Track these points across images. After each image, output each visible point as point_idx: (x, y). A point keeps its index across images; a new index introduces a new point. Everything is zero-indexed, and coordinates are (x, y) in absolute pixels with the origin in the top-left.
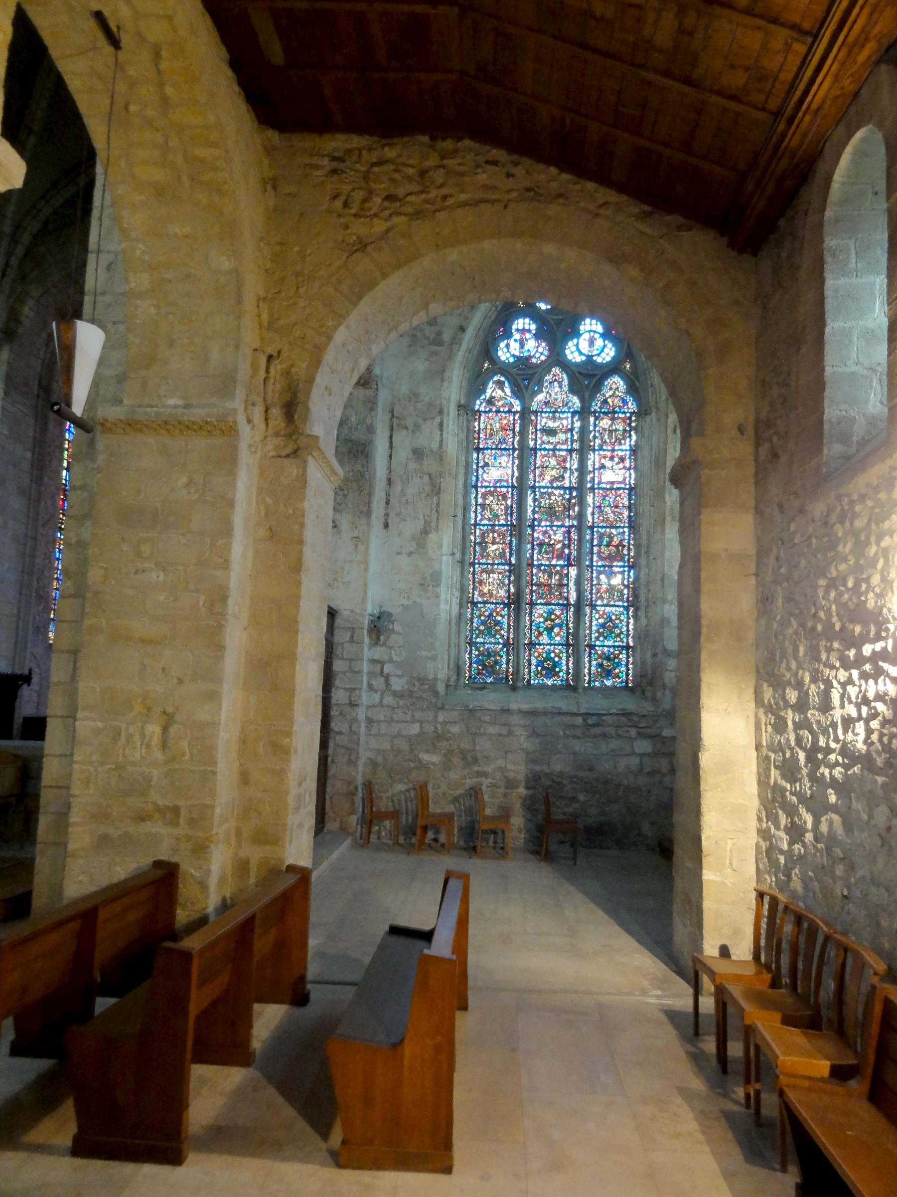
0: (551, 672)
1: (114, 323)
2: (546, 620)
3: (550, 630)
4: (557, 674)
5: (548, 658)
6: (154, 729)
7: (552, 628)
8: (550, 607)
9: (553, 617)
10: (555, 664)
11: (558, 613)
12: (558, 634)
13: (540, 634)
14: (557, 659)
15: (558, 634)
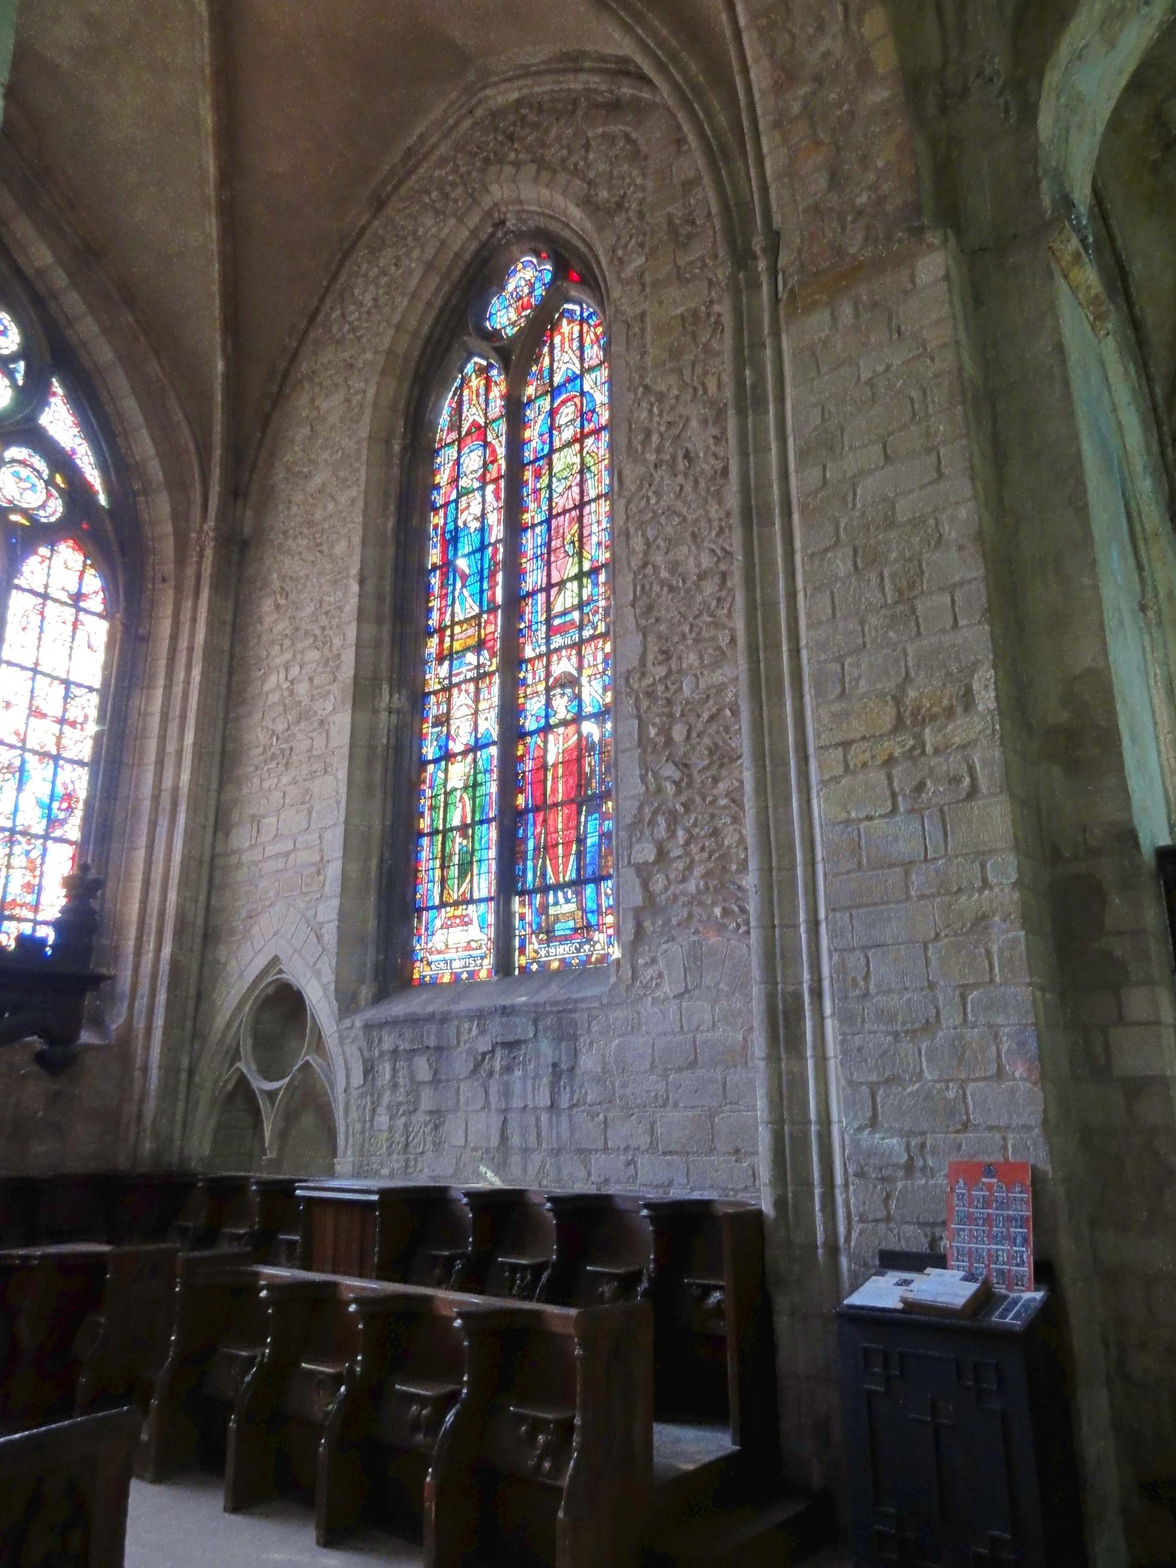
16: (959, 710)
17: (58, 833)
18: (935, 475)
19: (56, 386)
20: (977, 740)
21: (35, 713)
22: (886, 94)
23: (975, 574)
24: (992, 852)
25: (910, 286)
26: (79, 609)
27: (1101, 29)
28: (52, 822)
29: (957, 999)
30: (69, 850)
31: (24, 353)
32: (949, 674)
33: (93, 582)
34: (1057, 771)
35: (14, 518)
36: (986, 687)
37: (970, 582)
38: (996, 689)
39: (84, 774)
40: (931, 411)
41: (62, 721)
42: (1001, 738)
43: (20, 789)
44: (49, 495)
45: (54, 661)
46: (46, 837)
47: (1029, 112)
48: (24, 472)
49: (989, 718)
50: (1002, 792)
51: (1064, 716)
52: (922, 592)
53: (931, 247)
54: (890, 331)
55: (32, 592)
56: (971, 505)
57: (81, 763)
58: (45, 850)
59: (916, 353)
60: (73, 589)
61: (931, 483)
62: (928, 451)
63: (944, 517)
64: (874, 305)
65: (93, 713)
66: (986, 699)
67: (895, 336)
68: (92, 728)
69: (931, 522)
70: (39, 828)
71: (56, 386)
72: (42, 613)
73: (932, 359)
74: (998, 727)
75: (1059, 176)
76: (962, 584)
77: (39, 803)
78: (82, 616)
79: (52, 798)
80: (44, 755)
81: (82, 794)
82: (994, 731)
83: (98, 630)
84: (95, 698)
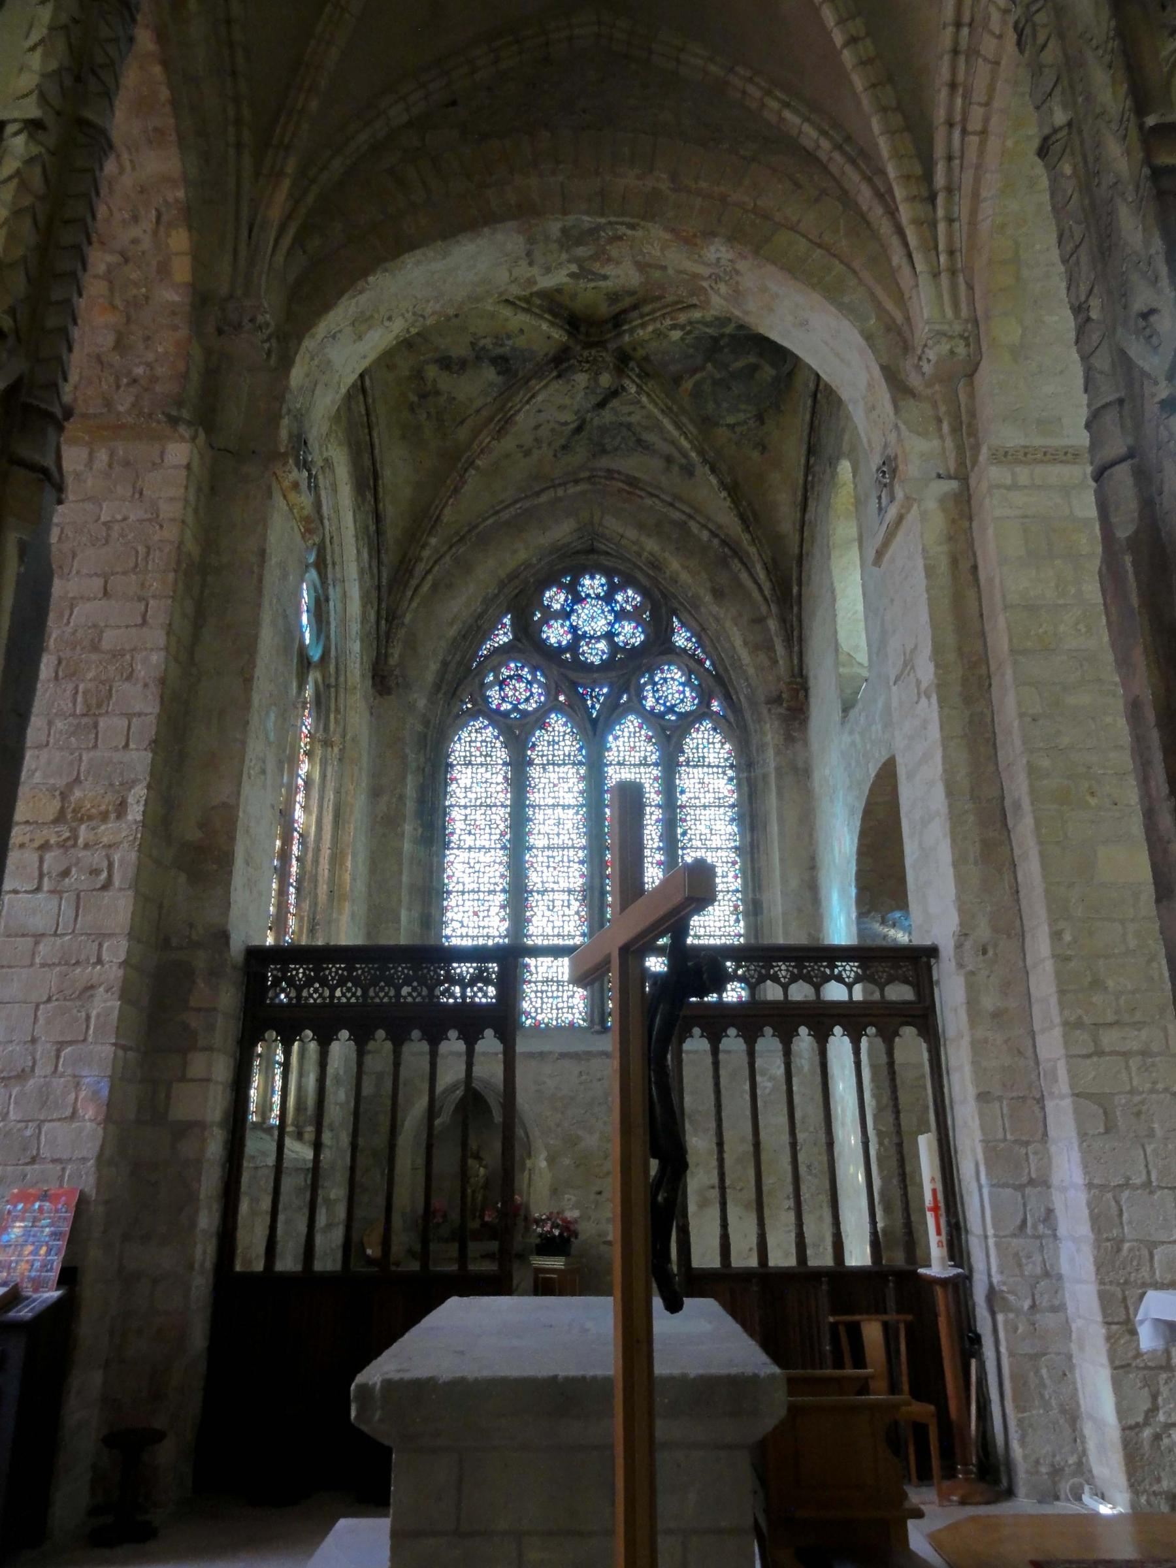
16: (113, 816)
18: (139, 621)
20: (121, 842)
22: (177, 298)
23: (150, 710)
24: (111, 935)
25: (158, 461)
27: (353, 324)
29: (53, 1054)
32: (111, 785)
34: (183, 878)
36: (138, 802)
37: (146, 715)
38: (146, 804)
40: (150, 568)
42: (140, 845)
47: (286, 362)
49: (134, 827)
50: (130, 888)
51: (199, 834)
52: (107, 712)
53: (182, 439)
54: (134, 488)
56: (163, 654)
59: (149, 516)
61: (136, 625)
62: (140, 599)
63: (139, 657)
64: (127, 463)
66: (135, 813)
67: (137, 496)
69: (128, 657)
73: (161, 527)
74: (139, 836)
75: (299, 417)
76: (140, 715)
82: (135, 838)
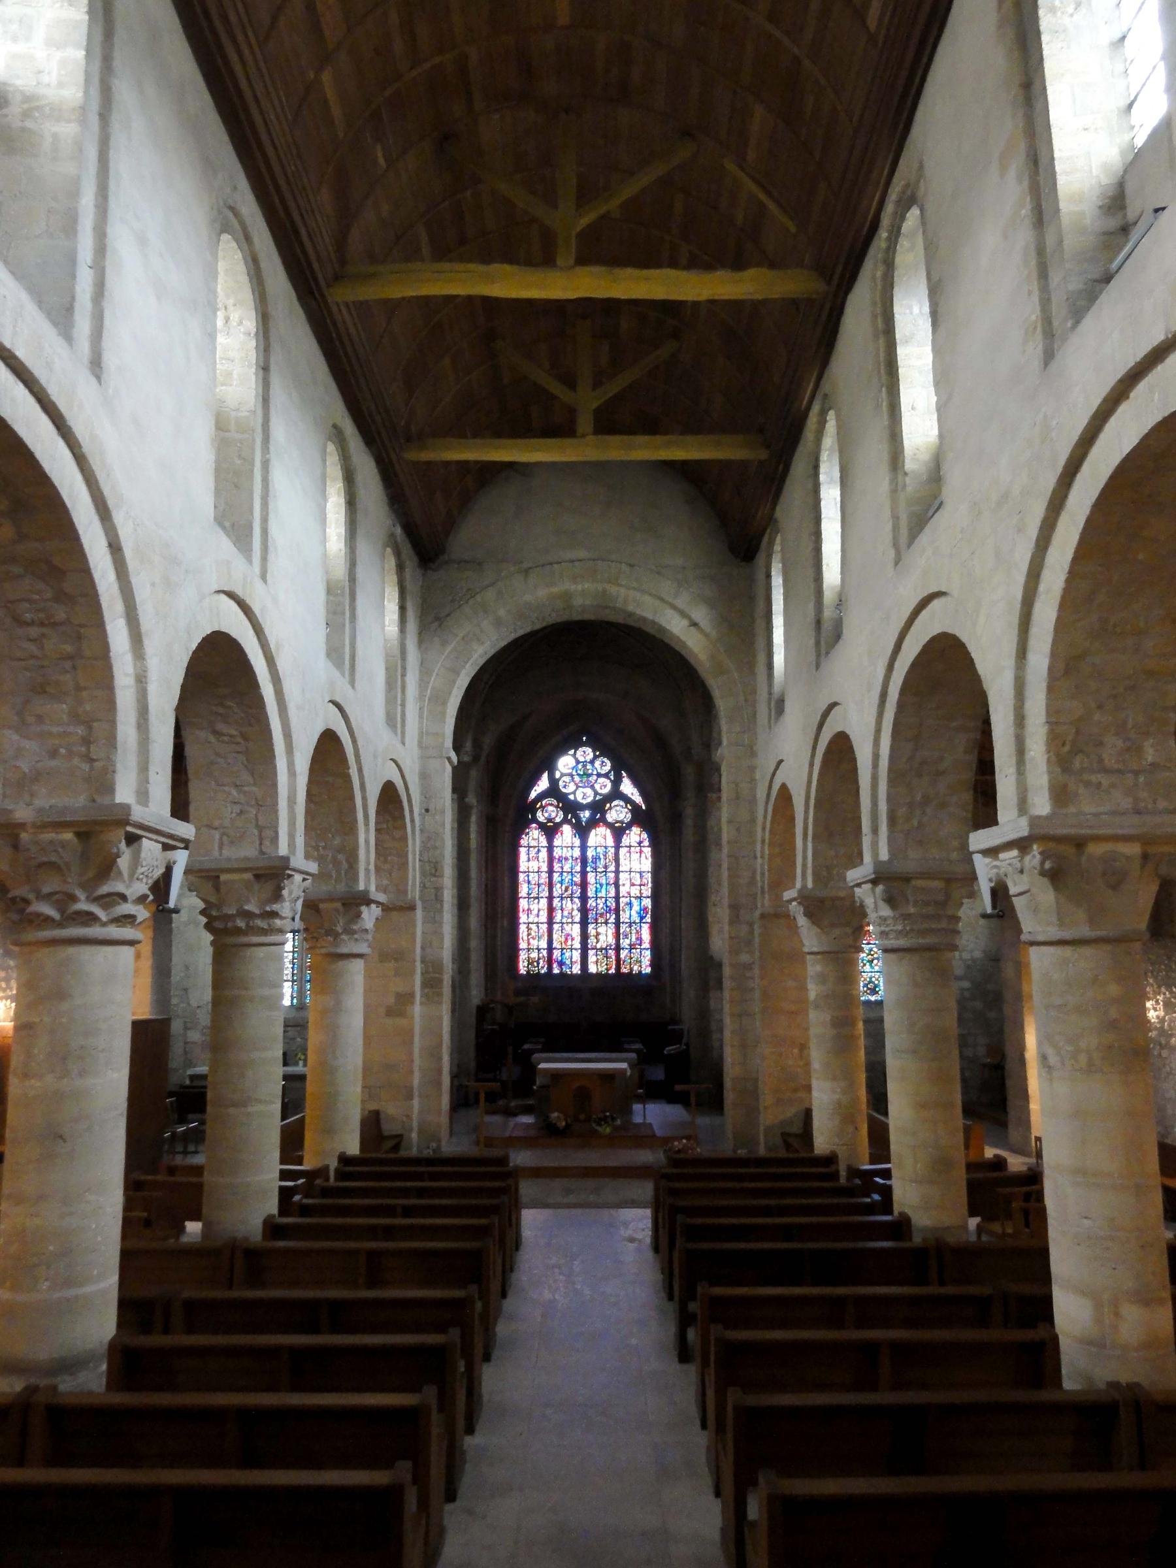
0: (874, 991)
1: (743, 857)
2: (868, 955)
3: (871, 962)
4: (877, 993)
5: (870, 982)
6: (796, 1051)
7: (872, 961)
8: (870, 946)
9: (872, 953)
10: (876, 986)
11: (875, 950)
12: (876, 965)
13: (865, 965)
14: (876, 982)
15: (876, 965)
17: (644, 921)
19: (624, 774)
21: (633, 885)
26: (640, 846)
28: (642, 918)
30: (648, 925)
31: (613, 768)
33: (645, 836)
35: (617, 825)
39: (649, 900)
41: (640, 885)
43: (631, 910)
44: (627, 813)
45: (636, 866)
46: (640, 923)
48: (618, 808)
55: (626, 846)
57: (648, 897)
58: (641, 926)
60: (638, 839)
65: (650, 880)
68: (650, 885)
70: (638, 921)
71: (624, 774)
72: (630, 852)
77: (637, 913)
78: (643, 849)
79: (641, 910)
80: (636, 898)
81: (650, 907)
83: (648, 851)
84: (650, 875)
